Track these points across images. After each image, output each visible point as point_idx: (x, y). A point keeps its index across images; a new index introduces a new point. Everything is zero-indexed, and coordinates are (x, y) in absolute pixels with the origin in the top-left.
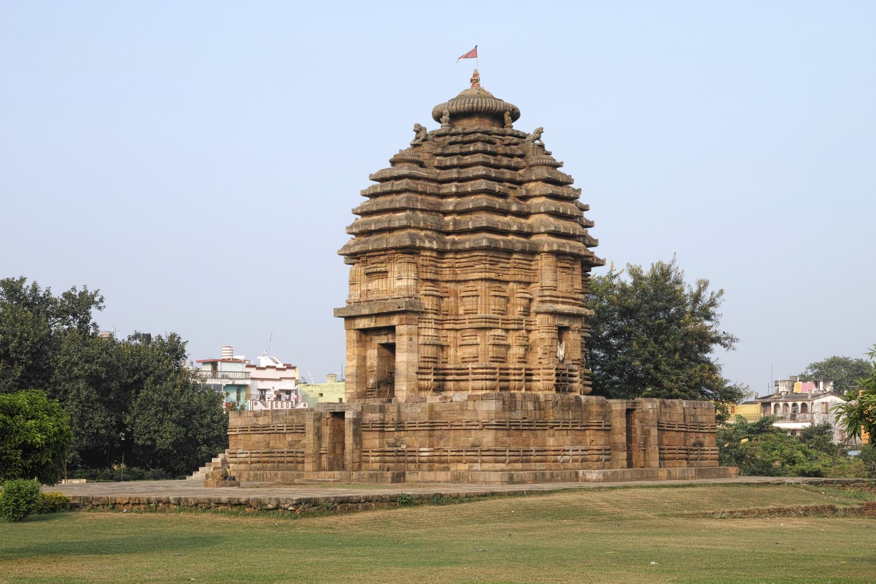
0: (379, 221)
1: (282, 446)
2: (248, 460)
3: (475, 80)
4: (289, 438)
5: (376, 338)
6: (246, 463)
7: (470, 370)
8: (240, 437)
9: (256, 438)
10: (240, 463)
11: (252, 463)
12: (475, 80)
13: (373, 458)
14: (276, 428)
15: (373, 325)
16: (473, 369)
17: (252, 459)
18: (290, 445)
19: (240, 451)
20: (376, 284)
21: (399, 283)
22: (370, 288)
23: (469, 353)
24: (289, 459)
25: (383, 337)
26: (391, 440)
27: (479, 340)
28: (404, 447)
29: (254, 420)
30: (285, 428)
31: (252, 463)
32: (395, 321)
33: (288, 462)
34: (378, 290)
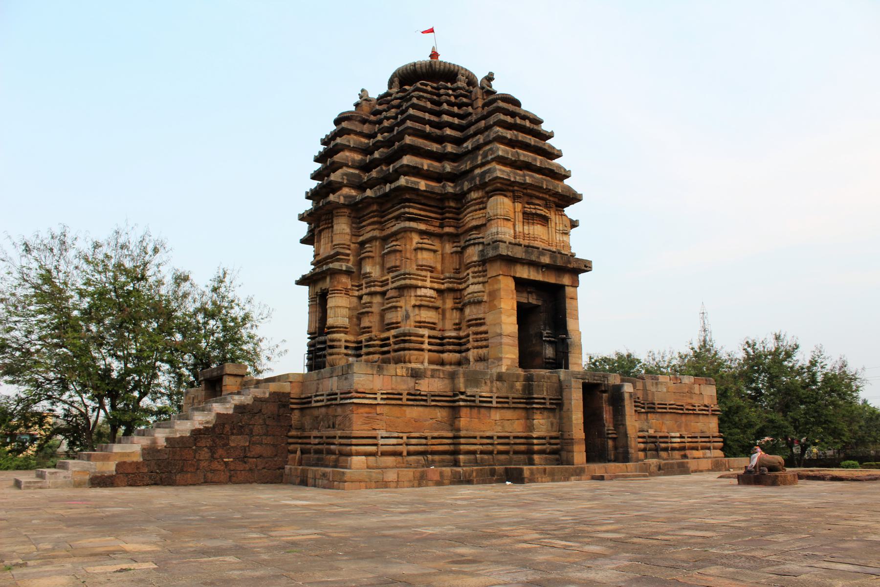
0: (528, 156)
2: (404, 449)
3: (434, 55)
6: (400, 454)
8: (379, 409)
9: (413, 413)
10: (384, 454)
11: (409, 454)
12: (434, 55)
14: (478, 399)
17: (412, 448)
19: (385, 434)
20: (538, 230)
22: (526, 232)
28: (651, 432)
29: (411, 382)
30: (494, 400)
31: (409, 454)
33: (500, 453)
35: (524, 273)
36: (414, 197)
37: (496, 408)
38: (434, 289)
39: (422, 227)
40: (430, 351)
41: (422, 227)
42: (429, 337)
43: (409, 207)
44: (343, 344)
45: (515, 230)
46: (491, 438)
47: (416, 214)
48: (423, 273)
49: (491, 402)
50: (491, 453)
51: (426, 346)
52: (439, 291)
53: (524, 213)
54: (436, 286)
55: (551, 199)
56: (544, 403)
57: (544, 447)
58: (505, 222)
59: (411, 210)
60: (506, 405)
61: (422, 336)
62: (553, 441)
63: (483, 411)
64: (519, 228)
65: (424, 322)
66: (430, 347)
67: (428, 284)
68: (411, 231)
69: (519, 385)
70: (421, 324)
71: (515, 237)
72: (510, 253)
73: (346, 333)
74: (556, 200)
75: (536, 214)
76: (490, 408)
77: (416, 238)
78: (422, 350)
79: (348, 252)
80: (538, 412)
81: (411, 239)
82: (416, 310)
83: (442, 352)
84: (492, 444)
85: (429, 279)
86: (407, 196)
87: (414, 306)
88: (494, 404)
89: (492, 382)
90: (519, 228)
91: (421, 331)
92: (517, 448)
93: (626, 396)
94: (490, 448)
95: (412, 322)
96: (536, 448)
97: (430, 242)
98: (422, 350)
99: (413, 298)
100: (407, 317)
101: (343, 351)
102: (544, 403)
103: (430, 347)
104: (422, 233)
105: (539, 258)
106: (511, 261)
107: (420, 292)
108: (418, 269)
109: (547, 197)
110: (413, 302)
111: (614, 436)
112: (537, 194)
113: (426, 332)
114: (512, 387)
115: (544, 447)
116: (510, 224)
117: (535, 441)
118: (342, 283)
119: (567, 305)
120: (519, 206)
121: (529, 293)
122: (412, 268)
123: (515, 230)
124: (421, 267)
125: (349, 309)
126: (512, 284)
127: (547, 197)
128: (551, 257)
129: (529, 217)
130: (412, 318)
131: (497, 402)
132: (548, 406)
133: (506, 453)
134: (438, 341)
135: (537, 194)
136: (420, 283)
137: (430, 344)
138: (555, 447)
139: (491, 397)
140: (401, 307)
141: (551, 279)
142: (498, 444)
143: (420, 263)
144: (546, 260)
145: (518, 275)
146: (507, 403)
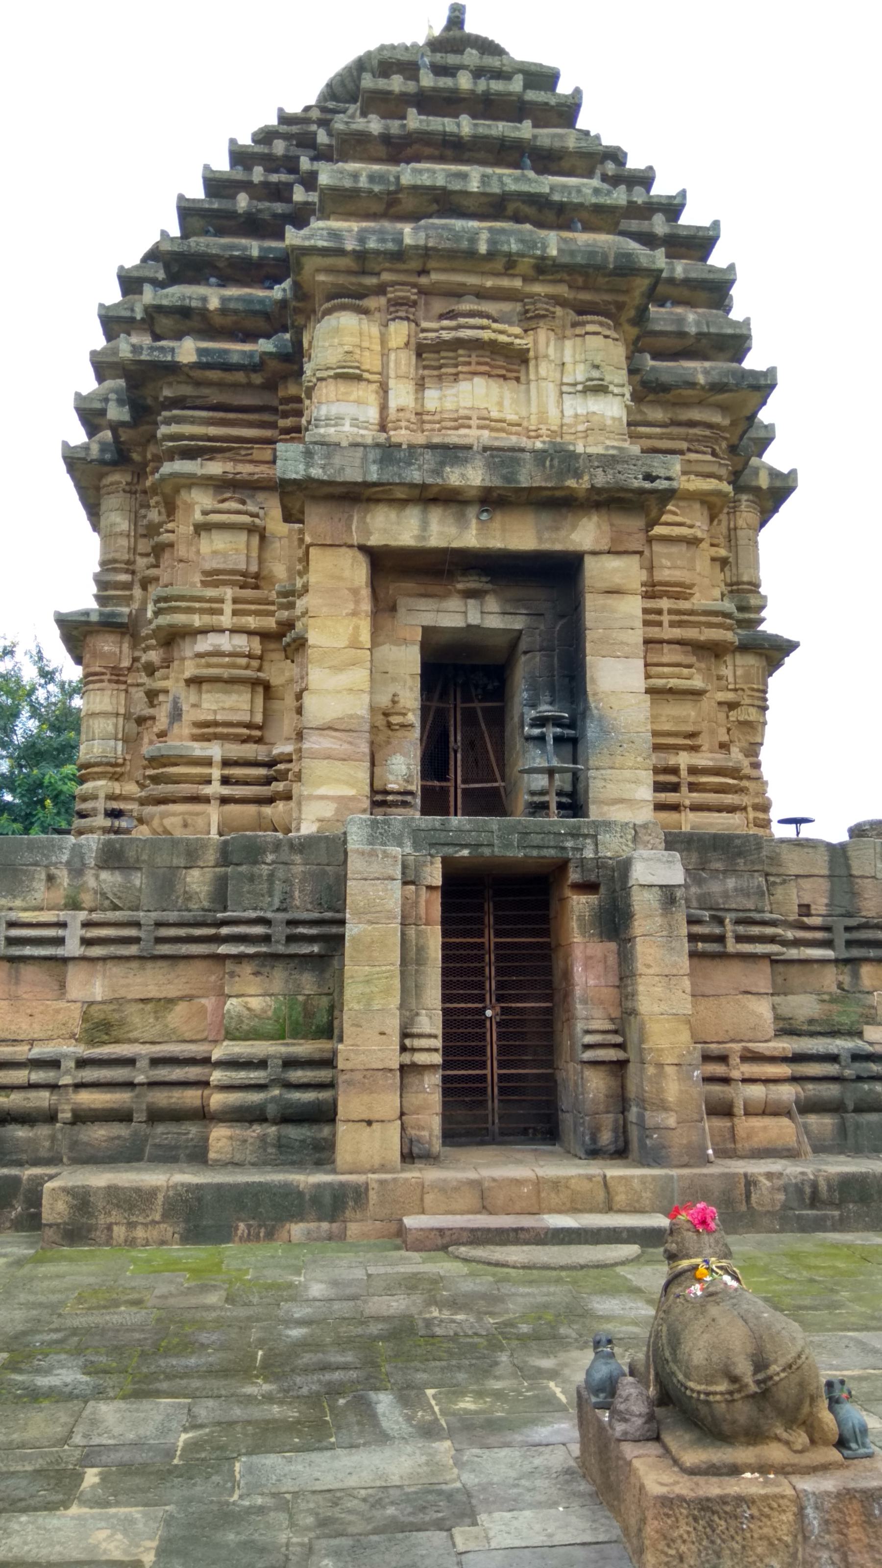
1: (24, 1027)
4: (91, 987)
5: (423, 604)
7: (684, 773)
13: (756, 1092)
15: (471, 535)
16: (693, 770)
18: (100, 1026)
21: (577, 407)
23: (677, 720)
24: (88, 1099)
25: (454, 603)
26: (804, 1006)
27: (697, 683)
32: (584, 534)
33: (81, 1117)
34: (487, 422)
35: (403, 529)
36: (187, 390)
37: (83, 958)
38: (250, 633)
39: (215, 468)
40: (225, 800)
41: (215, 468)
42: (226, 763)
43: (178, 420)
44: (100, 805)
45: (384, 407)
46: (54, 1064)
47: (192, 438)
48: (210, 592)
49: (59, 941)
50: (51, 1117)
51: (215, 789)
52: (265, 636)
53: (421, 350)
54: (252, 622)
55: (538, 288)
56: (266, 939)
57: (255, 1097)
58: (343, 387)
59: (174, 429)
60: (133, 950)
61: (208, 762)
62: (298, 1075)
63: (28, 972)
64: (402, 395)
65: (216, 724)
66: (226, 791)
67: (226, 620)
68: (189, 487)
69: (198, 881)
70: (208, 731)
71: (383, 428)
72: (316, 472)
73: (116, 777)
74: (562, 290)
75: (459, 343)
76: (65, 960)
77: (201, 501)
78: (206, 800)
79: (124, 577)
80: (247, 969)
81: (189, 507)
82: (193, 689)
83: (270, 801)
84: (53, 1087)
85: (228, 608)
86: (167, 392)
87: (190, 682)
88: (72, 948)
89: (77, 870)
90: (402, 395)
91: (199, 749)
92: (162, 1098)
93: (644, 903)
94: (42, 1099)
95: (184, 729)
96: (217, 1100)
97: (234, 505)
98: (206, 800)
99: (188, 663)
100: (176, 715)
101: (101, 821)
102: (266, 939)
103: (226, 791)
104: (224, 486)
105: (438, 472)
106: (353, 496)
107: (204, 644)
108: (204, 584)
109: (518, 283)
110: (190, 669)
111: (611, 1054)
112: (472, 280)
113: (215, 751)
114: (166, 884)
115: (255, 1097)
116: (368, 393)
117: (217, 1076)
118: (103, 655)
119: (591, 616)
120: (399, 332)
121: (469, 594)
122: (191, 583)
123: (384, 407)
124: (213, 577)
125: (127, 717)
126: (357, 571)
127: (518, 283)
128: (491, 466)
129: (436, 358)
130: (185, 717)
131: (87, 942)
132: (281, 949)
133: (123, 1116)
134: (262, 771)
135: (472, 280)
136: (197, 621)
137: (226, 781)
138: (309, 1096)
139: (63, 925)
140: (166, 692)
141: (520, 535)
142: (79, 1086)
143: (208, 566)
144: (473, 476)
145: (374, 541)
146: (136, 940)
